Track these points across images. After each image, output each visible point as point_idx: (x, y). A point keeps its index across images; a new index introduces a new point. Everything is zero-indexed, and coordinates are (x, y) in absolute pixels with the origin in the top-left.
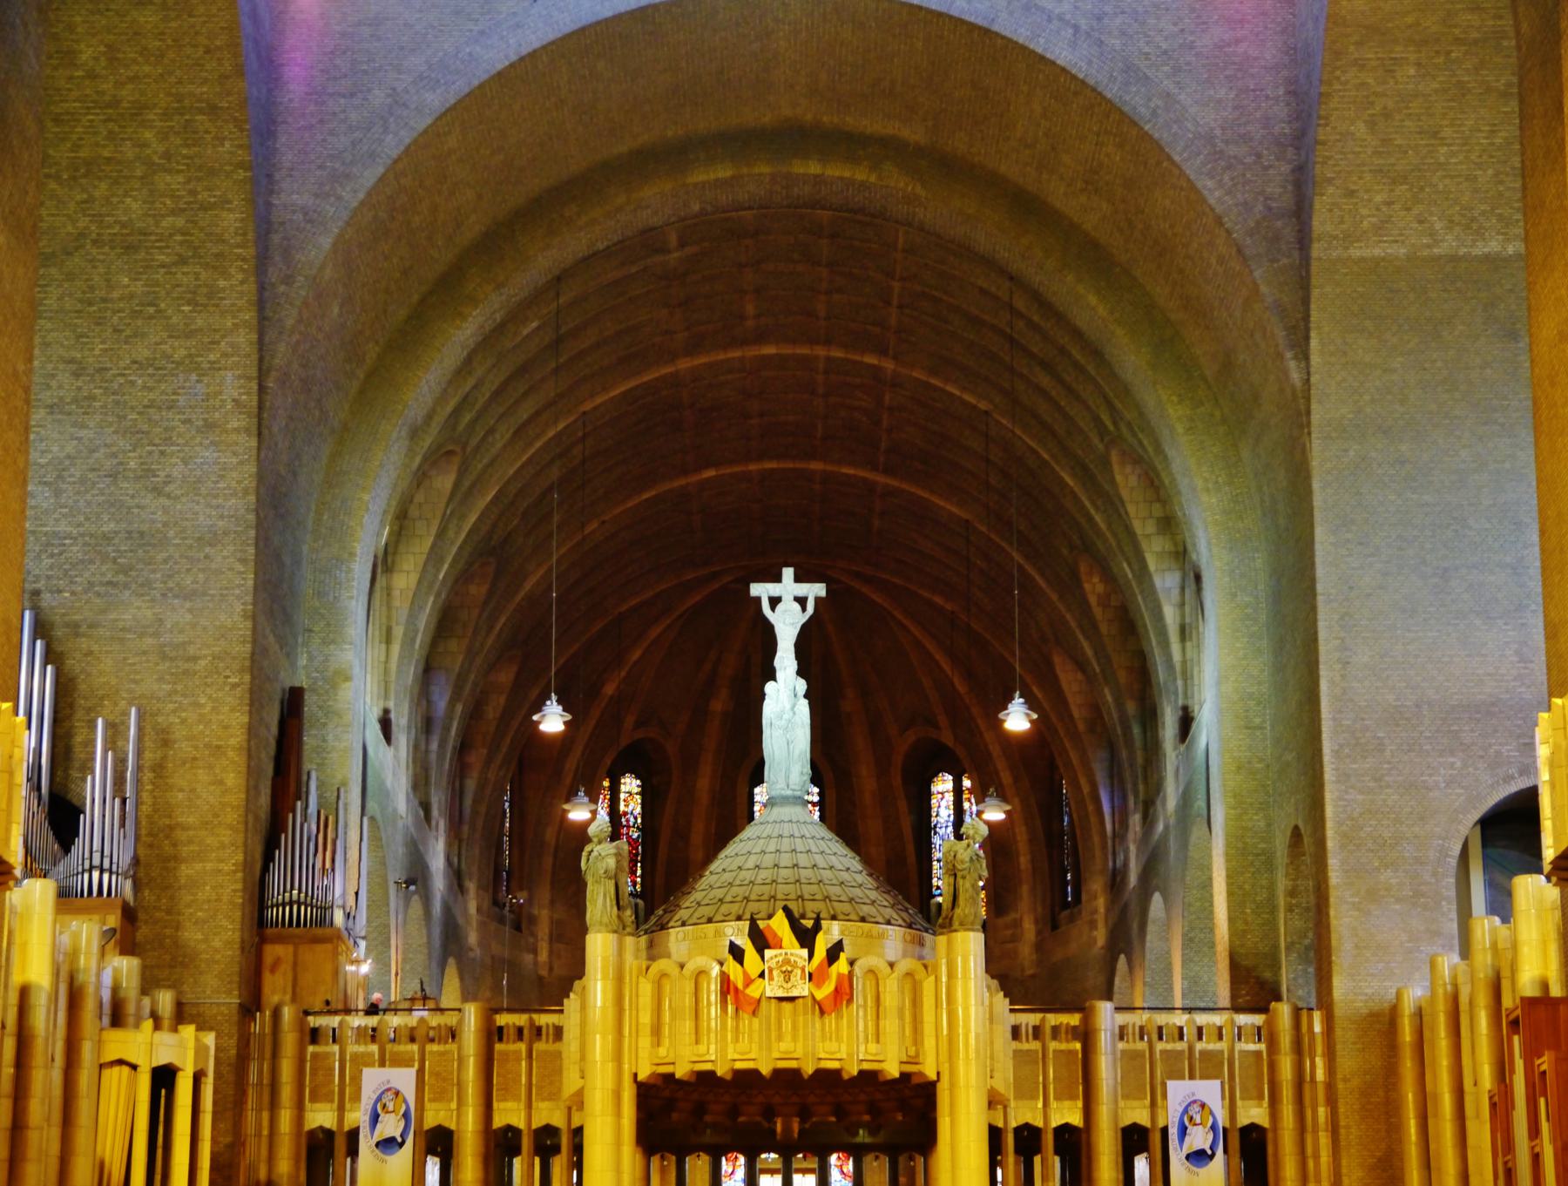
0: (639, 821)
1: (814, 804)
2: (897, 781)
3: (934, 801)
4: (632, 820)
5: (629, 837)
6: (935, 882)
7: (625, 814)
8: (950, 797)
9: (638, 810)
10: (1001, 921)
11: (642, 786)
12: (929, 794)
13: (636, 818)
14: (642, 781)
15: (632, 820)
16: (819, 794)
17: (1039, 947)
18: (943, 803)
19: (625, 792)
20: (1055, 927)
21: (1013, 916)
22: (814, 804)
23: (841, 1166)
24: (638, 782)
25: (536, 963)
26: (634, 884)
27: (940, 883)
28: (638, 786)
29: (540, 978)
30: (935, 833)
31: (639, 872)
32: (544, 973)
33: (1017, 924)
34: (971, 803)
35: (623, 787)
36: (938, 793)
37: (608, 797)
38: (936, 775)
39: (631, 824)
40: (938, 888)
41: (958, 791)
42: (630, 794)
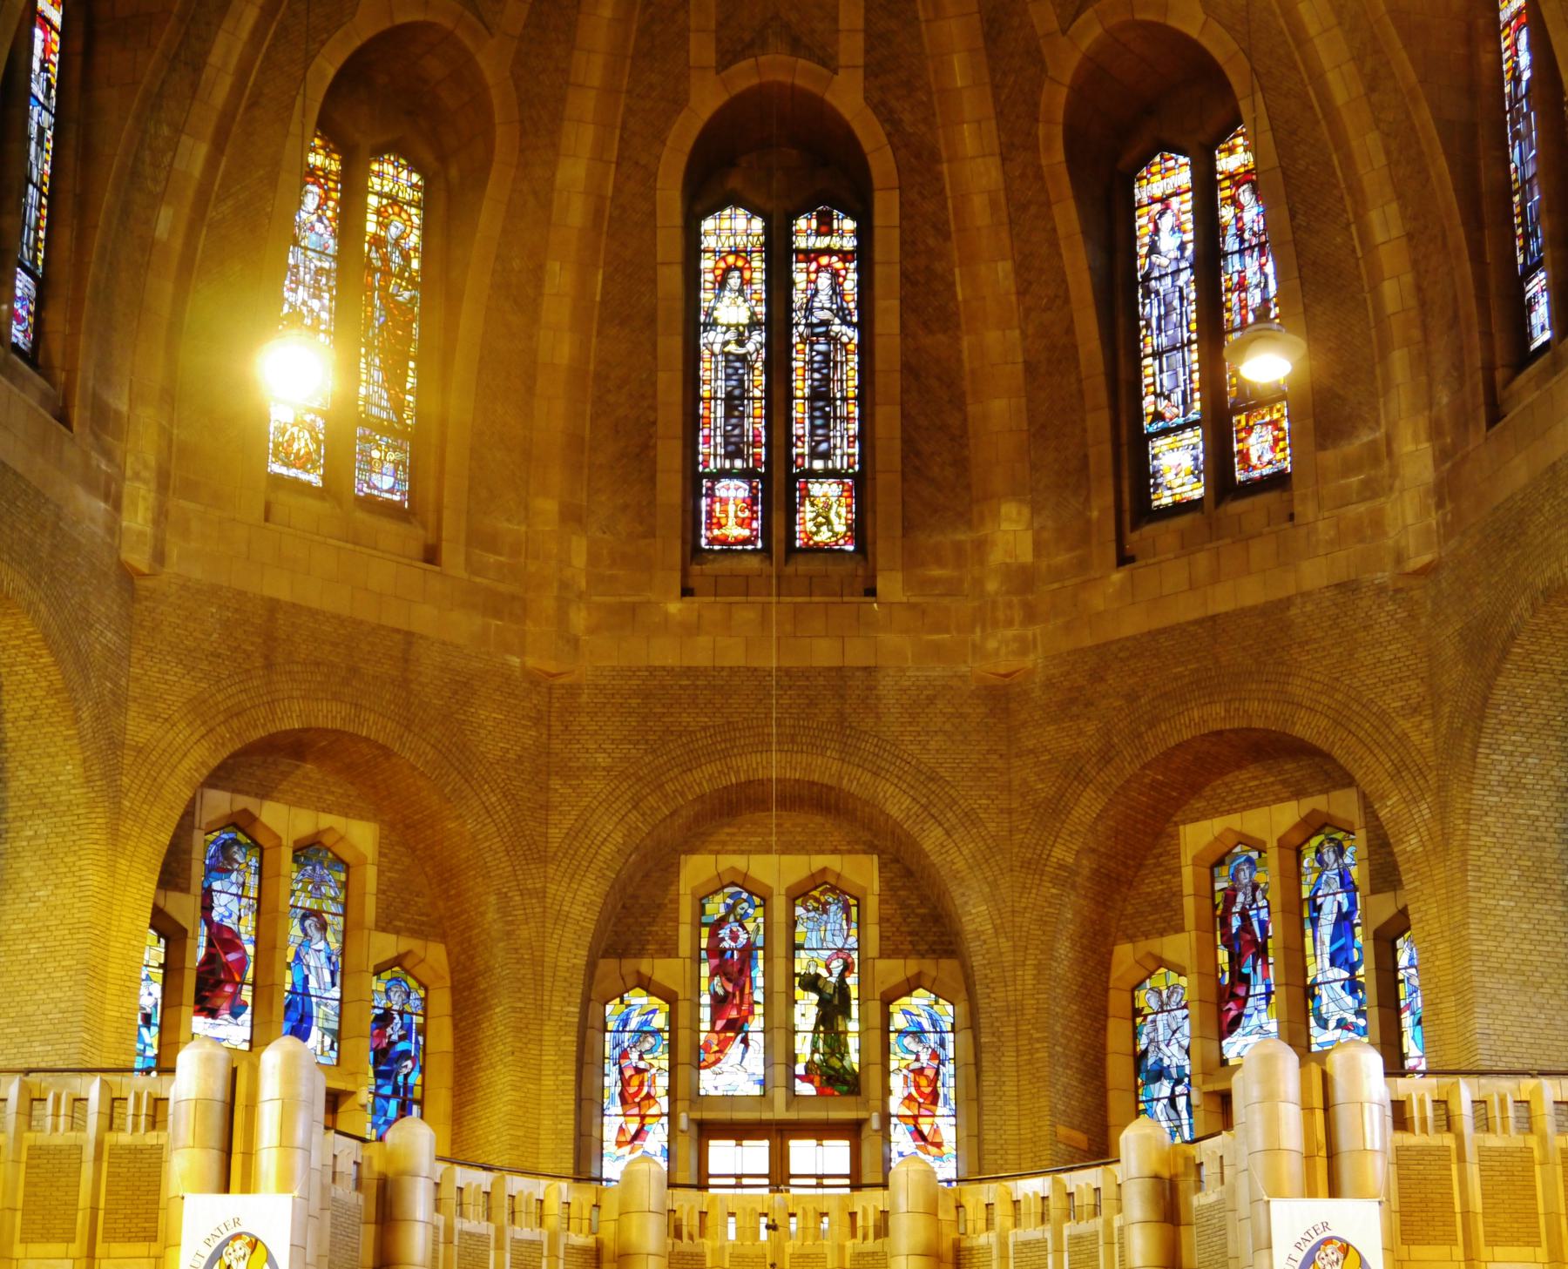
0: (415, 264)
1: (844, 256)
2: (1055, 157)
3: (1143, 223)
4: (396, 258)
5: (388, 298)
6: (1148, 404)
7: (378, 242)
8: (1184, 205)
9: (414, 239)
10: (1330, 457)
11: (427, 189)
12: (1130, 207)
13: (406, 257)
14: (424, 176)
15: (396, 258)
16: (859, 233)
17: (1445, 490)
18: (1166, 222)
19: (380, 195)
20: (1495, 415)
21: (1365, 437)
22: (844, 256)
23: (915, 1117)
24: (415, 178)
25: (113, 529)
26: (399, 408)
27: (1162, 405)
28: (413, 186)
29: (128, 577)
30: (1147, 294)
31: (411, 382)
32: (139, 559)
33: (1380, 454)
34: (1241, 207)
35: (375, 182)
36: (1153, 201)
37: (335, 195)
38: (1146, 161)
39: (394, 268)
40: (1158, 416)
41: (1205, 188)
42: (394, 200)
